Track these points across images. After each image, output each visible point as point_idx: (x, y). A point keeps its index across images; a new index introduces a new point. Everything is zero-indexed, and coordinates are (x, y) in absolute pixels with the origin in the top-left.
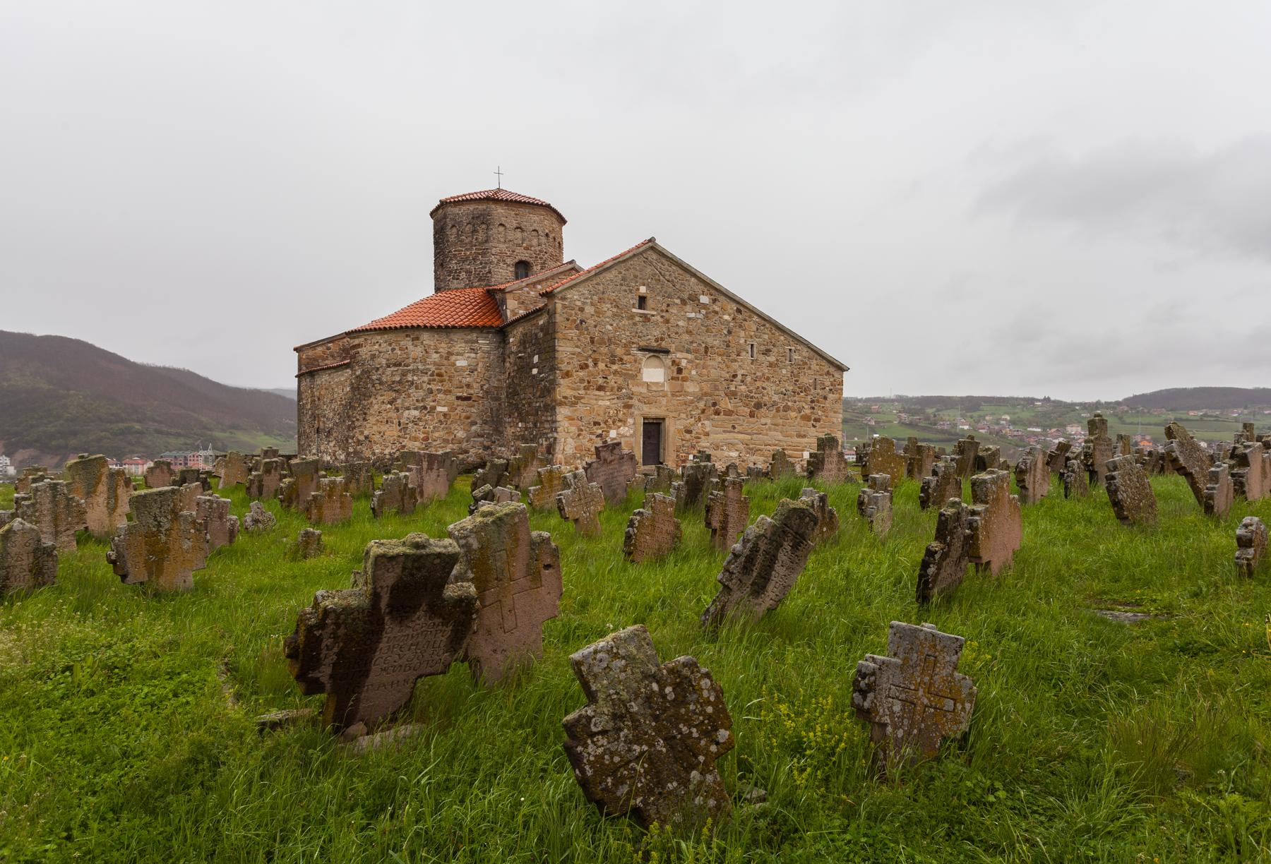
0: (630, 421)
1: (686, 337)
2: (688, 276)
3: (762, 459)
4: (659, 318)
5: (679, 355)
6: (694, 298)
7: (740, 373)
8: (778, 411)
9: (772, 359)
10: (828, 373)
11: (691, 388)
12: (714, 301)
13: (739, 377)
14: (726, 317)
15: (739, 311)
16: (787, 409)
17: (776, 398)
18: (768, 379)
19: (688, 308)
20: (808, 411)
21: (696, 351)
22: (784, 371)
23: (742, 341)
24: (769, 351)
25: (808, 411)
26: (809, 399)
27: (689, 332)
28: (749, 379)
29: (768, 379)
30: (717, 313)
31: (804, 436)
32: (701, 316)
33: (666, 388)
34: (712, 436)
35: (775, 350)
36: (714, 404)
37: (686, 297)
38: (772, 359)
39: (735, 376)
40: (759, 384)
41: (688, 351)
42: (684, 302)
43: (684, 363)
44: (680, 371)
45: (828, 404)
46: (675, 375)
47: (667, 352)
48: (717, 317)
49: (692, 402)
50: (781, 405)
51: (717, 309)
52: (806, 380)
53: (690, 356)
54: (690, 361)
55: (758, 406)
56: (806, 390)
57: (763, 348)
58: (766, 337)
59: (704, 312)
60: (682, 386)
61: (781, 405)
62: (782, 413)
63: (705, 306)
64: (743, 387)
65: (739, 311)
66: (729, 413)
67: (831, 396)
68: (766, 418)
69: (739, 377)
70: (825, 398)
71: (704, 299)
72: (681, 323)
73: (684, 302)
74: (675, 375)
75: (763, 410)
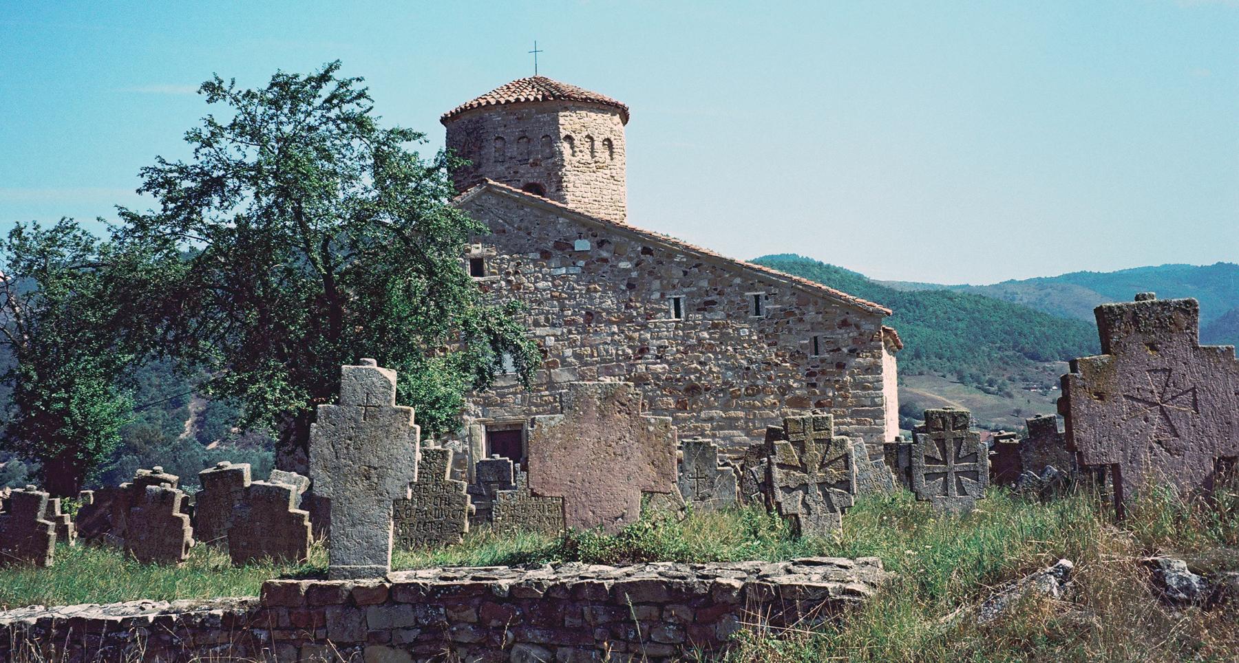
2: (552, 217)
4: (503, 283)
5: (539, 331)
6: (564, 246)
10: (845, 324)
12: (601, 244)
13: (654, 351)
14: (624, 265)
15: (646, 251)
18: (711, 348)
29: (711, 348)
30: (605, 260)
37: (551, 244)
39: (643, 350)
43: (551, 341)
48: (606, 268)
51: (605, 254)
58: (704, 284)
59: (582, 263)
63: (582, 254)
64: (659, 368)
65: (646, 251)
69: (654, 351)
71: (582, 245)
72: (541, 285)
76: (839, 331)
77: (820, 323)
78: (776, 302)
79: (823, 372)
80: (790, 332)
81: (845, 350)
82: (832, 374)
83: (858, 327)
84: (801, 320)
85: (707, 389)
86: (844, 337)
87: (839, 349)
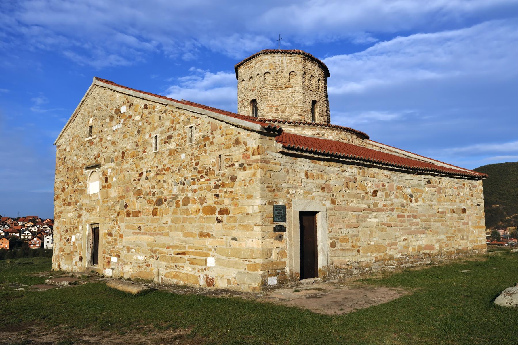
0: (80, 228)
1: (112, 148)
2: (116, 93)
3: (164, 264)
7: (144, 171)
8: (178, 205)
9: (172, 146)
10: (237, 142)
11: (113, 193)
16: (187, 201)
17: (175, 190)
18: (168, 169)
19: (114, 122)
20: (210, 201)
21: (117, 158)
22: (183, 156)
23: (147, 136)
24: (170, 137)
25: (210, 201)
26: (212, 184)
27: (113, 143)
28: (152, 174)
31: (208, 235)
32: (120, 126)
33: (99, 197)
34: (125, 238)
35: (176, 133)
36: (126, 206)
38: (172, 146)
39: (141, 174)
40: (159, 178)
41: (112, 161)
42: (112, 118)
44: (106, 180)
45: (237, 188)
46: (104, 184)
47: (98, 166)
49: (113, 206)
50: (181, 197)
52: (209, 161)
53: (113, 165)
54: (113, 169)
55: (159, 202)
56: (210, 172)
57: (165, 136)
60: (108, 192)
61: (181, 197)
62: (182, 207)
65: (146, 107)
66: (137, 214)
67: (241, 175)
68: (166, 217)
70: (233, 179)
73: (112, 118)
74: (104, 184)
75: (164, 206)
76: (233, 149)
77: (223, 144)
78: (200, 131)
79: (223, 185)
80: (206, 152)
81: (237, 165)
82: (228, 186)
83: (245, 144)
84: (212, 143)
85: (166, 200)
86: (236, 153)
87: (233, 165)
